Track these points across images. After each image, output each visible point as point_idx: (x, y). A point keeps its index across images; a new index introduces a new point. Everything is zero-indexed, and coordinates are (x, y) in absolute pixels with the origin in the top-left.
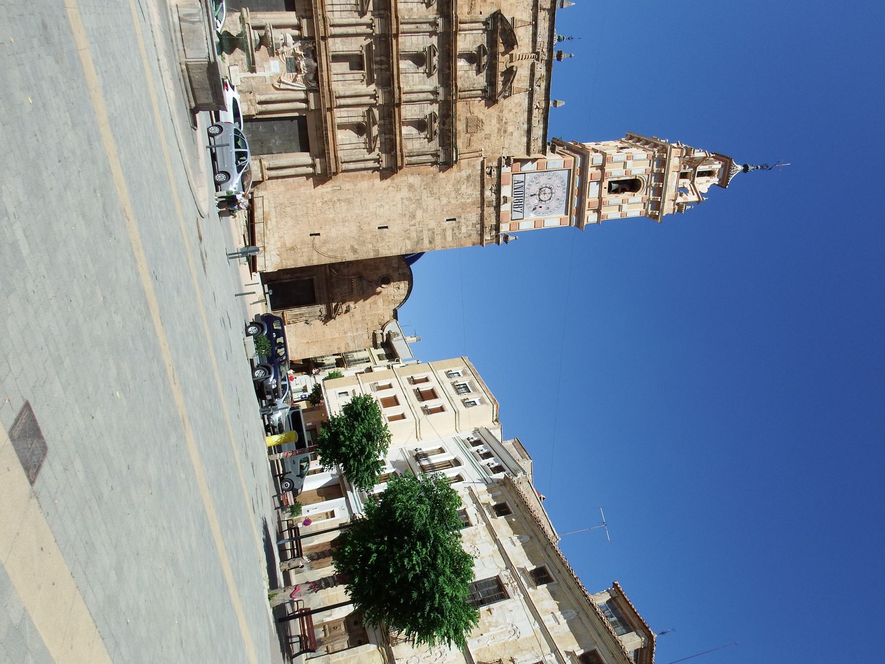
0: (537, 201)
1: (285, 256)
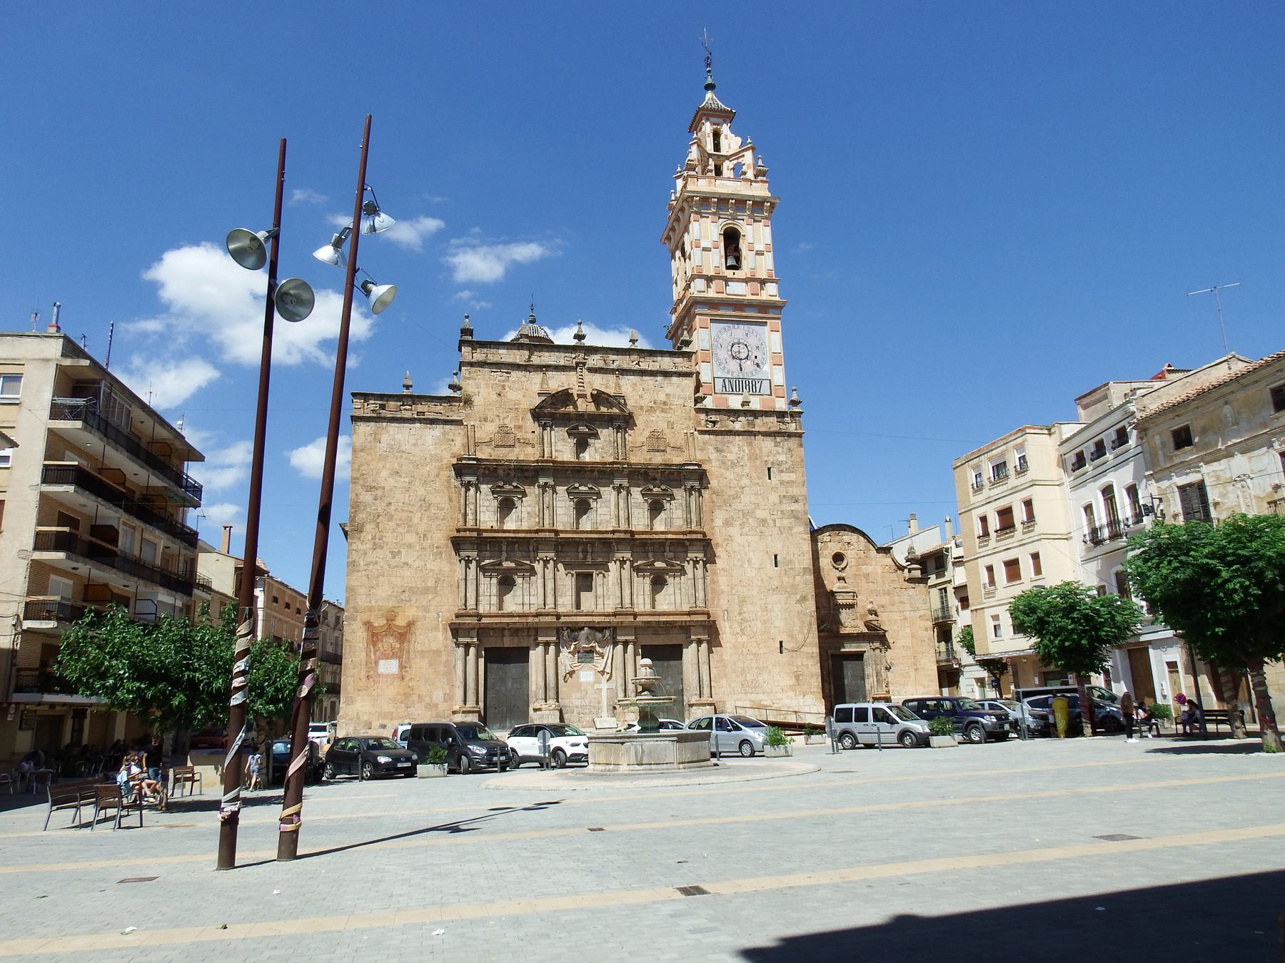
0: (749, 362)
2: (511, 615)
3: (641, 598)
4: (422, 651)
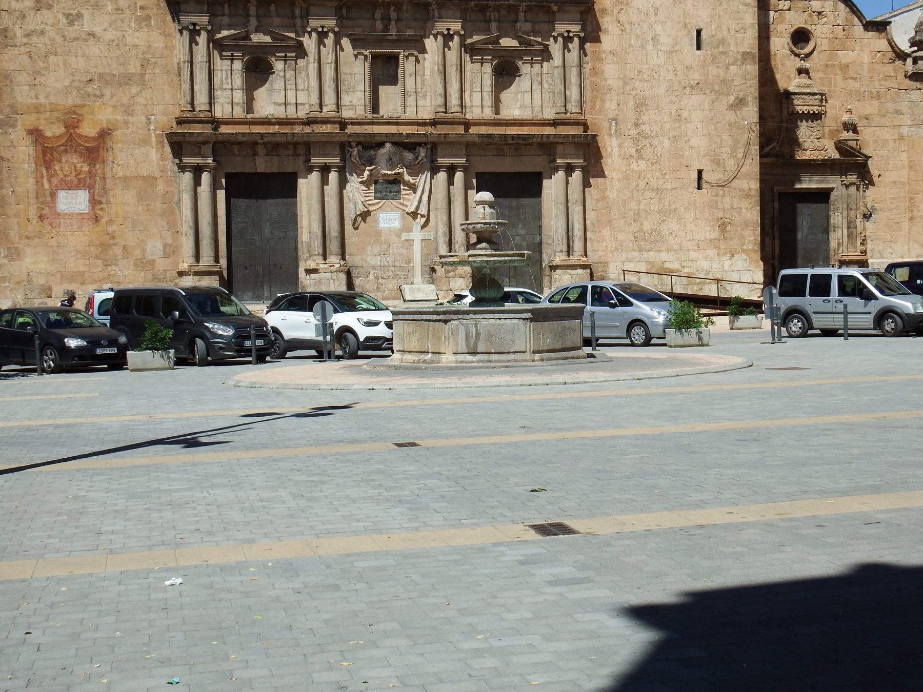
1: (735, 243)
2: (266, 122)
4: (126, 179)
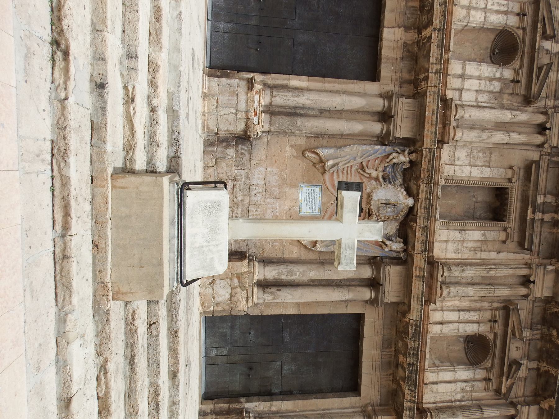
3: (451, 317)
